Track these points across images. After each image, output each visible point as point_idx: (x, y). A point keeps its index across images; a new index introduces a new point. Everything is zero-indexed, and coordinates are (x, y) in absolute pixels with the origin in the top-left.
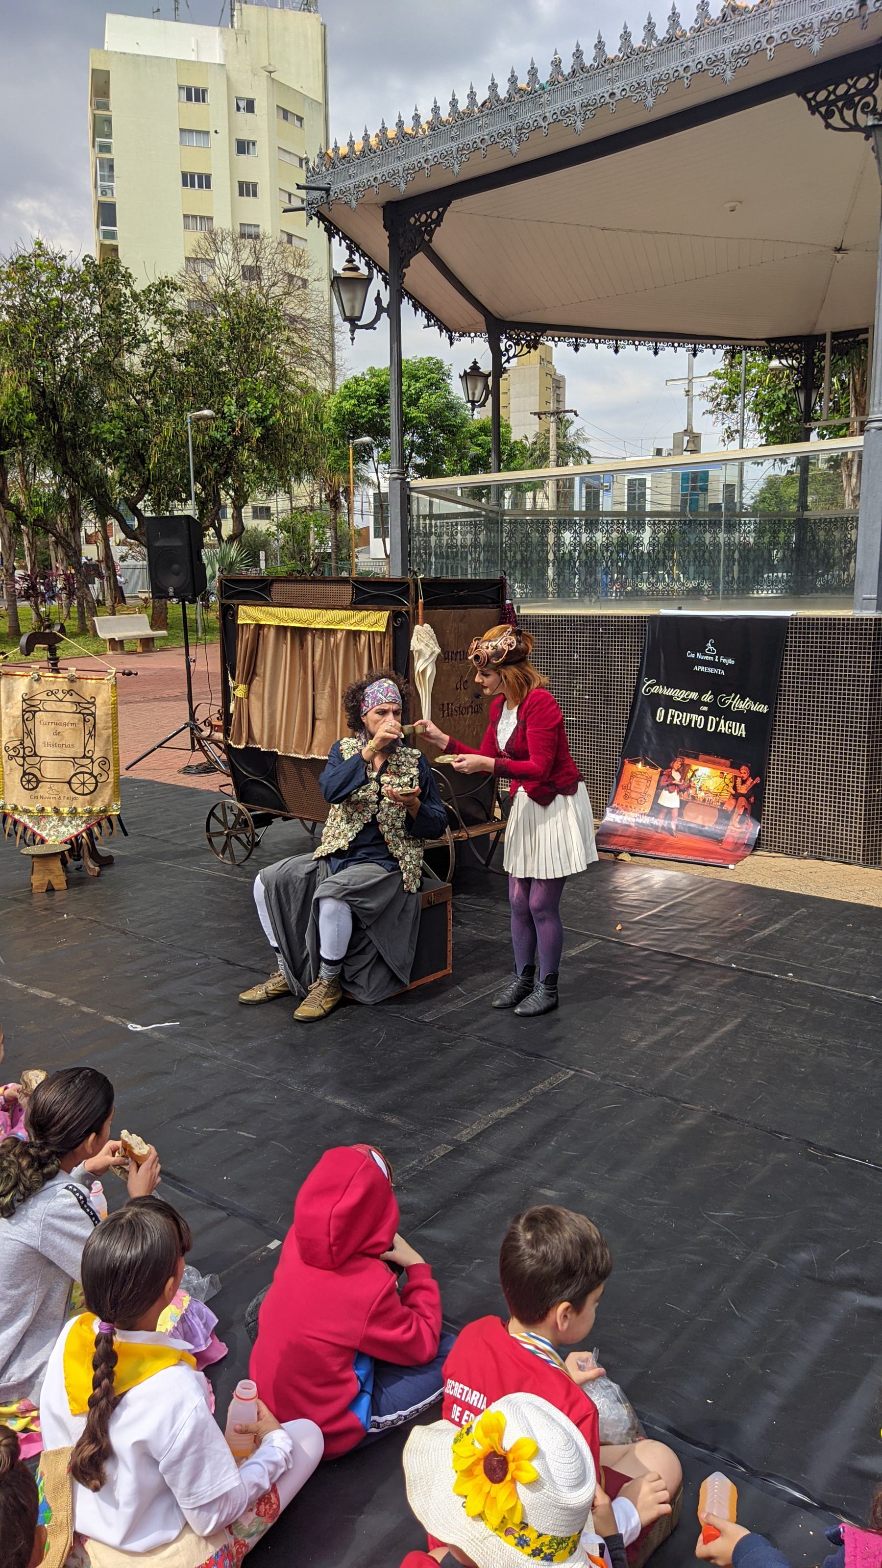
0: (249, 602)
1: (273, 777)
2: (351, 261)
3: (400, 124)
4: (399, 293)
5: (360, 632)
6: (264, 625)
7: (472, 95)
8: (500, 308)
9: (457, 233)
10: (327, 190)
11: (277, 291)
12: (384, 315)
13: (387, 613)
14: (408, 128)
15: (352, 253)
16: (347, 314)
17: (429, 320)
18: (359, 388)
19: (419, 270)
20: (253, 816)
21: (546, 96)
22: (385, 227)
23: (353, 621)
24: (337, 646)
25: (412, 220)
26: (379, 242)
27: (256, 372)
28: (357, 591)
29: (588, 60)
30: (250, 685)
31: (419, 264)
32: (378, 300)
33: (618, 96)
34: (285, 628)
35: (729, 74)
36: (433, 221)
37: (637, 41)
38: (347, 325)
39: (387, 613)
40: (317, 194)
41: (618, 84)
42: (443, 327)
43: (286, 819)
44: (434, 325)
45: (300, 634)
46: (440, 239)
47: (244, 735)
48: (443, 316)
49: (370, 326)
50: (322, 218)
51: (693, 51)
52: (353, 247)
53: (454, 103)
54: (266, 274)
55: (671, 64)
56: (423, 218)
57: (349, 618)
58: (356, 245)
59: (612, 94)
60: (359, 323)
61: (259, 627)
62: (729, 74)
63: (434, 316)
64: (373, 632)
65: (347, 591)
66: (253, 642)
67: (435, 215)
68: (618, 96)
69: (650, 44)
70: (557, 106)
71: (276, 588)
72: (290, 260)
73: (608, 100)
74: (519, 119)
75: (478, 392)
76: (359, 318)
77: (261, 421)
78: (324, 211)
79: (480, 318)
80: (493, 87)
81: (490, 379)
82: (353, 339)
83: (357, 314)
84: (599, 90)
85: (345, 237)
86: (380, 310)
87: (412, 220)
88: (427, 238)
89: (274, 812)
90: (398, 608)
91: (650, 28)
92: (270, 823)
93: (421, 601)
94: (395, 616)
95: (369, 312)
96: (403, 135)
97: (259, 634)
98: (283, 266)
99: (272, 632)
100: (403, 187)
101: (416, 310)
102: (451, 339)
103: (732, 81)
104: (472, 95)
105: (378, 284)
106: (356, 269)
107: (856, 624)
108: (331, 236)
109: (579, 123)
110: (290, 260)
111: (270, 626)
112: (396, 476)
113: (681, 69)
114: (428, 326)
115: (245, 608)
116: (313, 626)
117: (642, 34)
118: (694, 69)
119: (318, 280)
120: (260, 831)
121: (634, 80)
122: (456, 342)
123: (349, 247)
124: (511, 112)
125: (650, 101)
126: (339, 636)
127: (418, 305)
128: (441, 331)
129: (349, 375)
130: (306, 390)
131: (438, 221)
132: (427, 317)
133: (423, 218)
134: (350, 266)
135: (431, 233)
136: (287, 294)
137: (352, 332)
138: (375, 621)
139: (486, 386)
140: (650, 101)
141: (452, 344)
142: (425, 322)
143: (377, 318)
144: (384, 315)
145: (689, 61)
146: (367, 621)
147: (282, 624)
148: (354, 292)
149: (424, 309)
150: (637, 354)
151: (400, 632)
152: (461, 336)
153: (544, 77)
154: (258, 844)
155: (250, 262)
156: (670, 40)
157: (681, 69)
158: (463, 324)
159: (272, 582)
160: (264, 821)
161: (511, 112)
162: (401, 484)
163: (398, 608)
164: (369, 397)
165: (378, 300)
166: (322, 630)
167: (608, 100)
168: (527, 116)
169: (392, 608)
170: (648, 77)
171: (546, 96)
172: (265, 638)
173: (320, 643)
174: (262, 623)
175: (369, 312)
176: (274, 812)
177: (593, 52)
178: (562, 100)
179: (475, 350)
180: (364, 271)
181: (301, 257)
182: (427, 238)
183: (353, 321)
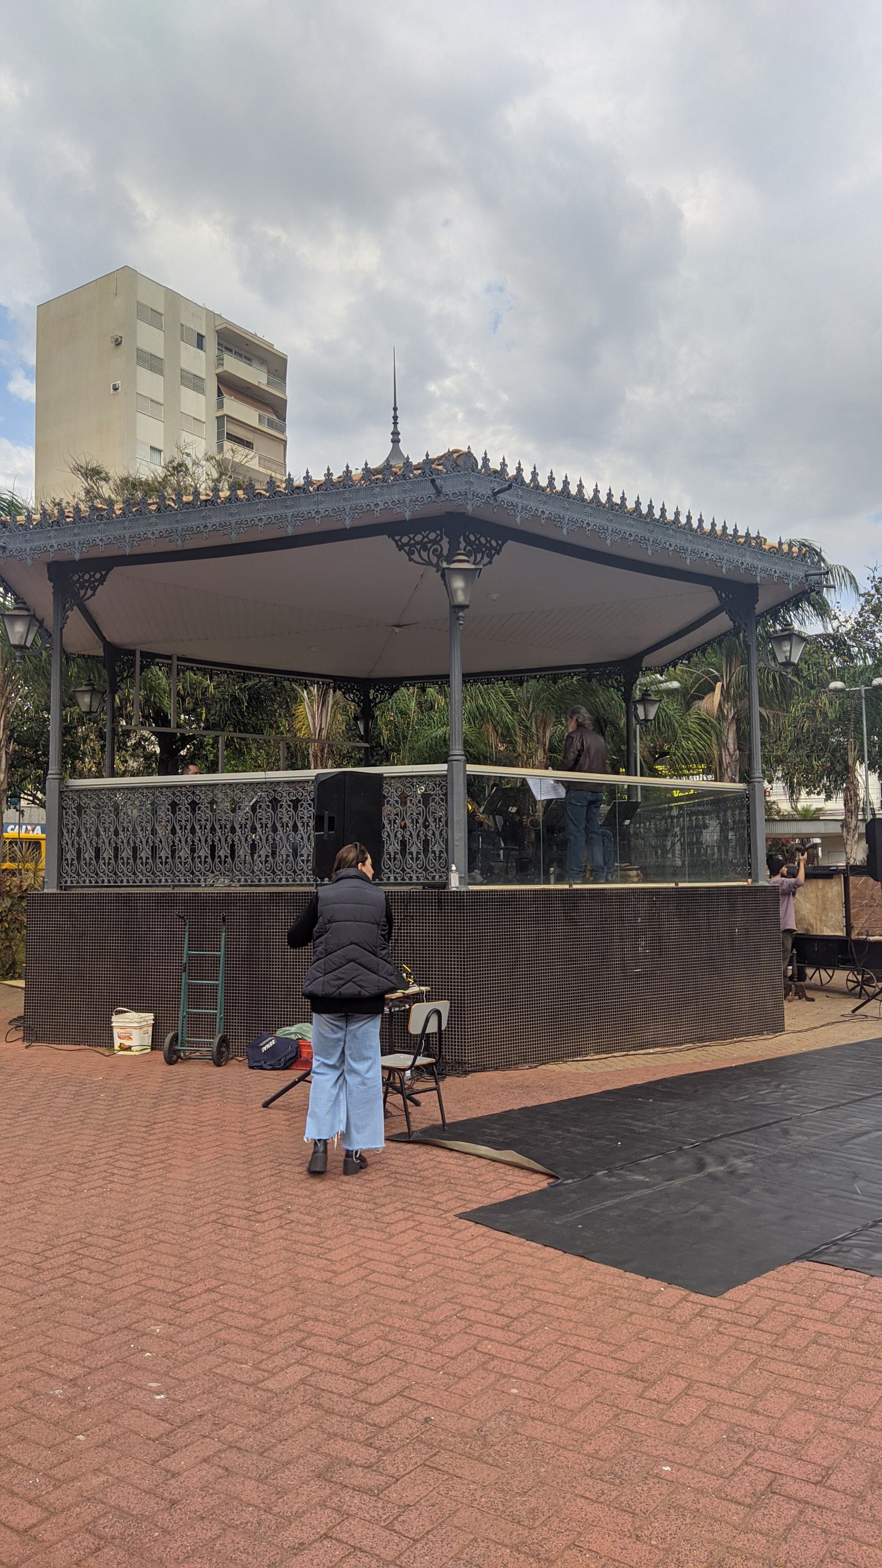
25: (76, 577)
36: (96, 580)
67: (98, 576)
87: (76, 577)
133: (87, 577)
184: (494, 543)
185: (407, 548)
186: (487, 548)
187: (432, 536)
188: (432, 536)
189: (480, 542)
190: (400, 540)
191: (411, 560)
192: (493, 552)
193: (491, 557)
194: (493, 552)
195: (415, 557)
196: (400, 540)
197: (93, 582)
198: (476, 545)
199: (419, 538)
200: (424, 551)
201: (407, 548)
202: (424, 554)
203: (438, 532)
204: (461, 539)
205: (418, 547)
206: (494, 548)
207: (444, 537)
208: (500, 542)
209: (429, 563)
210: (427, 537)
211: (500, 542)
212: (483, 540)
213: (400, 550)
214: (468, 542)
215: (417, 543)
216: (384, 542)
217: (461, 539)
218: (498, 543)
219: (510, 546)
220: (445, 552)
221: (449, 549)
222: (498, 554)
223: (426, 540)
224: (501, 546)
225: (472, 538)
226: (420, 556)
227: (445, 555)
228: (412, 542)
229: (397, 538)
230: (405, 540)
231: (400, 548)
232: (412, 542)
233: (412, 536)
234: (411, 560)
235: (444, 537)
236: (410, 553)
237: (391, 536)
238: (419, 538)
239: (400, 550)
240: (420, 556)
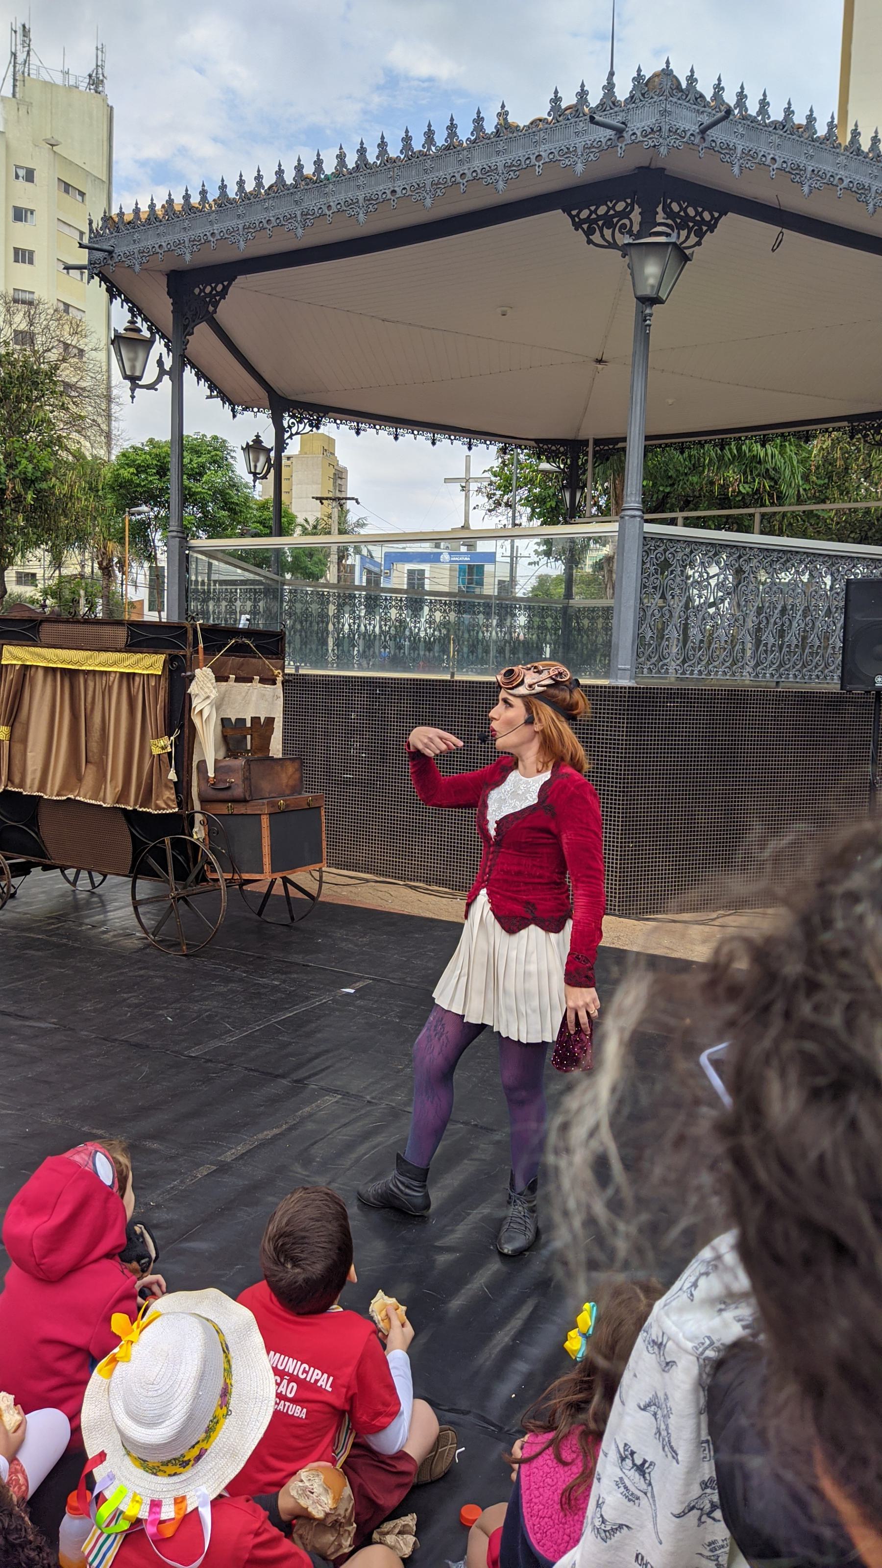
0: (15, 642)
1: (33, 822)
2: (132, 322)
3: (187, 197)
4: (182, 360)
5: (134, 674)
6: (31, 666)
7: (259, 178)
8: (280, 384)
9: (243, 306)
10: (110, 253)
11: (53, 356)
12: (166, 378)
13: (163, 656)
14: (195, 200)
15: (134, 316)
16: (128, 373)
17: (212, 391)
18: (138, 457)
19: (202, 338)
20: (11, 865)
21: (331, 186)
22: (168, 294)
23: (128, 663)
24: (110, 688)
25: (197, 291)
26: (163, 306)
27: (27, 433)
28: (132, 635)
29: (372, 157)
30: (12, 726)
31: (202, 330)
32: (160, 363)
33: (399, 194)
34: (54, 670)
35: (501, 185)
36: (218, 294)
37: (418, 145)
38: (128, 383)
39: (163, 656)
40: (100, 255)
41: (399, 183)
42: (225, 398)
43: (46, 868)
44: (217, 397)
45: (70, 675)
46: (225, 312)
47: (3, 778)
48: (226, 388)
49: (151, 387)
50: (104, 278)
51: (469, 160)
52: (136, 310)
53: (241, 183)
54: (39, 339)
55: (449, 169)
56: (208, 289)
57: (123, 660)
58: (138, 309)
59: (394, 192)
60: (140, 383)
61: (26, 668)
62: (501, 185)
63: (216, 387)
64: (148, 675)
65: (122, 634)
66: (17, 684)
67: (220, 288)
68: (399, 194)
69: (429, 149)
70: (342, 197)
71: (46, 628)
72: (67, 327)
73: (389, 196)
74: (305, 205)
75: (260, 465)
76: (140, 378)
77: (28, 482)
78: (108, 271)
79: (263, 394)
80: (280, 172)
81: (272, 454)
82: (133, 397)
83: (138, 374)
84: (381, 186)
85: (127, 300)
86: (162, 372)
87: (197, 291)
88: (211, 309)
89: (33, 859)
90: (175, 652)
91: (429, 135)
92: (29, 873)
93: (201, 645)
94: (171, 660)
95: (150, 374)
96: (188, 207)
97: (25, 675)
98: (58, 333)
99: (40, 673)
100: (188, 257)
101: (199, 379)
102: (233, 410)
103: (504, 191)
104: (259, 178)
105: (159, 347)
106: (138, 330)
107: (613, 691)
108: (112, 297)
109: (361, 215)
110: (67, 327)
111: (37, 667)
112: (174, 534)
113: (458, 176)
114: (211, 397)
115: (11, 648)
116: (83, 668)
117: (423, 140)
118: (469, 176)
119: (96, 350)
120: (16, 881)
121: (414, 181)
122: (238, 415)
123: (131, 310)
124: (297, 197)
125: (428, 202)
126: (112, 679)
127: (200, 375)
128: (224, 403)
129: (126, 445)
130: (79, 456)
131: (223, 294)
132: (209, 387)
133: (208, 289)
134: (132, 326)
135: (216, 304)
136: (64, 360)
137: (133, 390)
138: (151, 664)
139: (268, 460)
140: (428, 202)
141: (234, 416)
142: (208, 392)
143: (159, 380)
144: (166, 378)
145: (465, 168)
146: (141, 664)
147: (51, 665)
148: (136, 353)
149: (207, 379)
150: (414, 443)
151: (177, 680)
152: (244, 410)
153: (329, 168)
154: (13, 896)
155: (23, 326)
156: (448, 148)
157: (458, 176)
158: (247, 398)
159: (42, 621)
160: (22, 870)
161: (297, 197)
162: (180, 542)
163: (175, 652)
164: (148, 466)
165: (160, 363)
166: (94, 672)
167: (389, 196)
168: (312, 202)
169: (169, 651)
170: (428, 179)
171: (331, 186)
172: (32, 680)
173: (91, 684)
174: (28, 663)
175: (150, 374)
176: (33, 859)
177: (376, 151)
178: (346, 192)
179: (259, 424)
180: (146, 334)
181: (78, 326)
182: (211, 309)
183: (134, 380)
184: (707, 216)
185: (585, 226)
186: (696, 223)
187: (620, 206)
188: (620, 206)
189: (686, 212)
190: (578, 214)
191: (590, 242)
192: (705, 228)
193: (700, 235)
194: (705, 228)
195: (596, 238)
196: (578, 215)
197: (215, 295)
198: (681, 217)
199: (602, 210)
200: (608, 228)
201: (585, 226)
202: (607, 233)
203: (629, 201)
204: (660, 209)
205: (600, 223)
206: (707, 224)
207: (636, 206)
208: (716, 215)
209: (613, 245)
210: (613, 208)
211: (716, 215)
212: (691, 212)
213: (577, 229)
214: (670, 214)
215: (599, 217)
216: (558, 218)
217: (660, 209)
218: (712, 216)
219: (731, 222)
220: (636, 228)
221: (641, 224)
222: (712, 232)
223: (612, 212)
224: (717, 220)
225: (675, 207)
226: (603, 236)
227: (635, 232)
228: (594, 216)
229: (574, 213)
230: (585, 214)
231: (577, 226)
232: (594, 216)
233: (593, 208)
234: (590, 242)
235: (636, 206)
236: (589, 233)
237: (567, 210)
238: (602, 210)
239: (577, 229)
240: (603, 236)
